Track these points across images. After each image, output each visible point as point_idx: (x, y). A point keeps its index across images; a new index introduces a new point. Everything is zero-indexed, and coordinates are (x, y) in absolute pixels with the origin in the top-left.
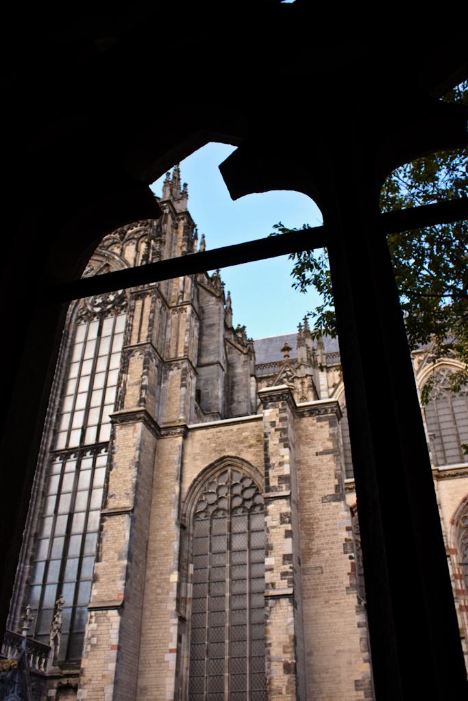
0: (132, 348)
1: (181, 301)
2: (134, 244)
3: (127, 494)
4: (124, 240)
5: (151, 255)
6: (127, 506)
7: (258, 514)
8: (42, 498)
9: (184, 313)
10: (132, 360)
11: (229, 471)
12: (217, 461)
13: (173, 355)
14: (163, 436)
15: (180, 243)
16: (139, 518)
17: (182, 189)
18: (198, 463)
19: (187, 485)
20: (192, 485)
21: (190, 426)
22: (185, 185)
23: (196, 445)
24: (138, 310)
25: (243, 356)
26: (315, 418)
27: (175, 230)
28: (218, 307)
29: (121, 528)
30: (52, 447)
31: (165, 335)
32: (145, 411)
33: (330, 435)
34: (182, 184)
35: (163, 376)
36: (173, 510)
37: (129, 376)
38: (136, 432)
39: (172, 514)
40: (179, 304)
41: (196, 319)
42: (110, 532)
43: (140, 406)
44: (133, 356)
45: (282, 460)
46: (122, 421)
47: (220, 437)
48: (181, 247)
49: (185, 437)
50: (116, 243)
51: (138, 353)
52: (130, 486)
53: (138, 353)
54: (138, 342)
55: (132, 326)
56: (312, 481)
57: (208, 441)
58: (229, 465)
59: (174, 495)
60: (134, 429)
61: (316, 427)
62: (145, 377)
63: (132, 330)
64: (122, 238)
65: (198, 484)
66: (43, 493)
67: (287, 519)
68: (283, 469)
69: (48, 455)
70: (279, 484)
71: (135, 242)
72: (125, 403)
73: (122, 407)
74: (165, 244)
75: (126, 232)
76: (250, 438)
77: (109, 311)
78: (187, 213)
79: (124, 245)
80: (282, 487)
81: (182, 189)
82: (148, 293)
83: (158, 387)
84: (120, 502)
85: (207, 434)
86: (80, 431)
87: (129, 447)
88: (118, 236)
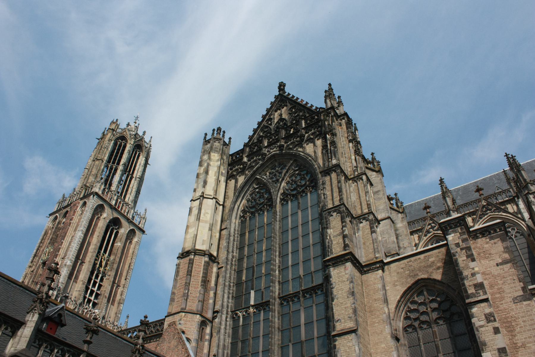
1: (356, 173)
3: (349, 317)
4: (304, 141)
5: (329, 145)
6: (352, 326)
7: (457, 321)
8: (279, 332)
13: (359, 212)
14: (365, 271)
16: (362, 335)
18: (398, 287)
19: (392, 306)
20: (397, 306)
21: (385, 261)
23: (393, 274)
24: (328, 183)
25: (400, 215)
26: (487, 237)
27: (340, 127)
28: (379, 178)
29: (351, 344)
30: (279, 294)
31: (351, 199)
33: (504, 248)
34: (337, 97)
35: (356, 228)
36: (386, 327)
38: (347, 270)
39: (386, 330)
40: (356, 176)
41: (370, 184)
42: (342, 349)
43: (345, 250)
44: (332, 216)
45: (473, 271)
46: (333, 264)
47: (411, 266)
48: (347, 138)
51: (335, 213)
52: (351, 311)
54: (333, 205)
55: (326, 194)
56: (500, 287)
57: (402, 270)
58: (423, 286)
59: (384, 315)
61: (490, 245)
63: (327, 198)
65: (401, 305)
66: (279, 328)
67: (492, 318)
68: (476, 278)
70: (476, 291)
72: (333, 251)
74: (336, 136)
76: (436, 262)
78: (346, 114)
80: (479, 293)
81: (338, 100)
83: (354, 236)
84: (346, 324)
85: (400, 265)
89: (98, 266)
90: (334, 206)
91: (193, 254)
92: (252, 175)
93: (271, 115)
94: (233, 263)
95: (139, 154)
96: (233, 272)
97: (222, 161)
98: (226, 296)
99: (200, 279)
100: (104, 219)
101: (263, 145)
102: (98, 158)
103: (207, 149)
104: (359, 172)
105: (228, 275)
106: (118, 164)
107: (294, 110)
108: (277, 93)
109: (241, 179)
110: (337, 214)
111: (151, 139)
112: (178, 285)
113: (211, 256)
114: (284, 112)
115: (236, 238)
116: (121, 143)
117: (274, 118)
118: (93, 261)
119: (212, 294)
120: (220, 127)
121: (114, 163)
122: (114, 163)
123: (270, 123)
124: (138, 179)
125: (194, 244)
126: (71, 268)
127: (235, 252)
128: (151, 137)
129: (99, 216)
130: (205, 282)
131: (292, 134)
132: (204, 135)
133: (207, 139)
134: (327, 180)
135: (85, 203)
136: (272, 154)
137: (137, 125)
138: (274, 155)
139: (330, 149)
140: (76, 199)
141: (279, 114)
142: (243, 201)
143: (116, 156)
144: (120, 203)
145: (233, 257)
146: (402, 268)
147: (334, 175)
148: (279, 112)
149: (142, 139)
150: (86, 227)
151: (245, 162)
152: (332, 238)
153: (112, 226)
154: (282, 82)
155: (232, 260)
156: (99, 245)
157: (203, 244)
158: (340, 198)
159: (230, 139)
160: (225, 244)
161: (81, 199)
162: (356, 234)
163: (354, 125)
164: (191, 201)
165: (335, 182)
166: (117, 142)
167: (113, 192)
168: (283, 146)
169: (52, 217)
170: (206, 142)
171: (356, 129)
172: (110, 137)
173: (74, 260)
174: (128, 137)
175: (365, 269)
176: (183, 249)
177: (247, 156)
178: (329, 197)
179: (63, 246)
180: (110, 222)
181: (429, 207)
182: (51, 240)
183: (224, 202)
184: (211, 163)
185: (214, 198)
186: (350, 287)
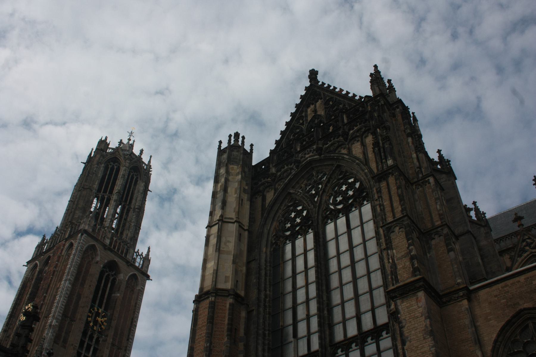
0: (390, 225)
1: (420, 175)
2: (358, 141)
4: (348, 141)
5: (381, 142)
9: (428, 185)
10: (393, 236)
11: (531, 325)
12: (514, 317)
13: (429, 225)
15: (402, 128)
17: (387, 85)
21: (471, 288)
22: (389, 81)
24: (384, 191)
32: (423, 279)
37: (394, 251)
43: (416, 276)
44: (393, 232)
48: (404, 131)
49: (469, 300)
50: (342, 145)
51: (397, 228)
53: (397, 228)
55: (383, 205)
57: (496, 298)
60: (417, 299)
62: (411, 247)
63: (384, 209)
64: (346, 139)
69: (329, 348)
71: (360, 139)
72: (399, 277)
73: (397, 281)
74: (389, 130)
75: (348, 133)
77: (352, 205)
79: (350, 144)
82: (390, 173)
86: (355, 319)
87: (417, 317)
88: (342, 139)
89: (91, 324)
90: (395, 219)
91: (214, 294)
92: (283, 189)
93: (302, 112)
94: (267, 304)
95: (137, 178)
96: (267, 316)
97: (243, 174)
98: (260, 348)
99: (226, 327)
100: (97, 263)
101: (296, 150)
102: (85, 187)
103: (224, 161)
104: (424, 174)
105: (261, 321)
106: (111, 192)
107: (331, 103)
108: (308, 84)
109: (270, 196)
110: (399, 229)
111: (150, 159)
112: (197, 337)
113: (237, 296)
114: (320, 107)
115: (268, 272)
116: (113, 166)
117: (306, 116)
118: (85, 318)
119: (241, 346)
120: (237, 133)
121: (105, 192)
122: (105, 192)
123: (301, 122)
124: (137, 210)
125: (214, 283)
126: (57, 329)
127: (268, 289)
128: (151, 157)
129: (90, 259)
130: (232, 330)
131: (331, 132)
132: (218, 144)
133: (222, 148)
134: (383, 186)
135: (71, 245)
136: (307, 160)
137: (131, 142)
138: (310, 162)
139: (384, 148)
140: (60, 240)
141: (313, 110)
142: (274, 224)
143: (108, 183)
144: (116, 241)
145: (266, 296)
146: (496, 296)
147: (391, 180)
148: (312, 107)
149: (139, 158)
150: (74, 274)
151: (273, 174)
152: (396, 262)
153: (107, 272)
154: (313, 70)
155: (265, 301)
156: (91, 297)
157: (226, 282)
158: (402, 208)
159: (252, 145)
160: (255, 281)
161: (66, 240)
162: (427, 255)
163: (412, 115)
164: (206, 228)
165: (393, 189)
166: (108, 165)
167: (106, 228)
168: (321, 149)
169: (32, 266)
170: (221, 152)
171: (415, 120)
172: (99, 159)
173: (60, 318)
174: (122, 159)
175: (444, 300)
176: (201, 289)
177: (275, 166)
178: (388, 209)
179: (46, 301)
180: (104, 267)
181: (521, 218)
182: (30, 294)
183: (250, 226)
184: (230, 178)
185: (236, 221)
186: (425, 325)
